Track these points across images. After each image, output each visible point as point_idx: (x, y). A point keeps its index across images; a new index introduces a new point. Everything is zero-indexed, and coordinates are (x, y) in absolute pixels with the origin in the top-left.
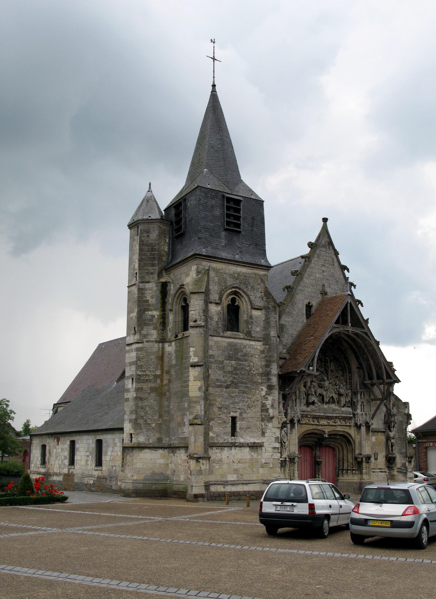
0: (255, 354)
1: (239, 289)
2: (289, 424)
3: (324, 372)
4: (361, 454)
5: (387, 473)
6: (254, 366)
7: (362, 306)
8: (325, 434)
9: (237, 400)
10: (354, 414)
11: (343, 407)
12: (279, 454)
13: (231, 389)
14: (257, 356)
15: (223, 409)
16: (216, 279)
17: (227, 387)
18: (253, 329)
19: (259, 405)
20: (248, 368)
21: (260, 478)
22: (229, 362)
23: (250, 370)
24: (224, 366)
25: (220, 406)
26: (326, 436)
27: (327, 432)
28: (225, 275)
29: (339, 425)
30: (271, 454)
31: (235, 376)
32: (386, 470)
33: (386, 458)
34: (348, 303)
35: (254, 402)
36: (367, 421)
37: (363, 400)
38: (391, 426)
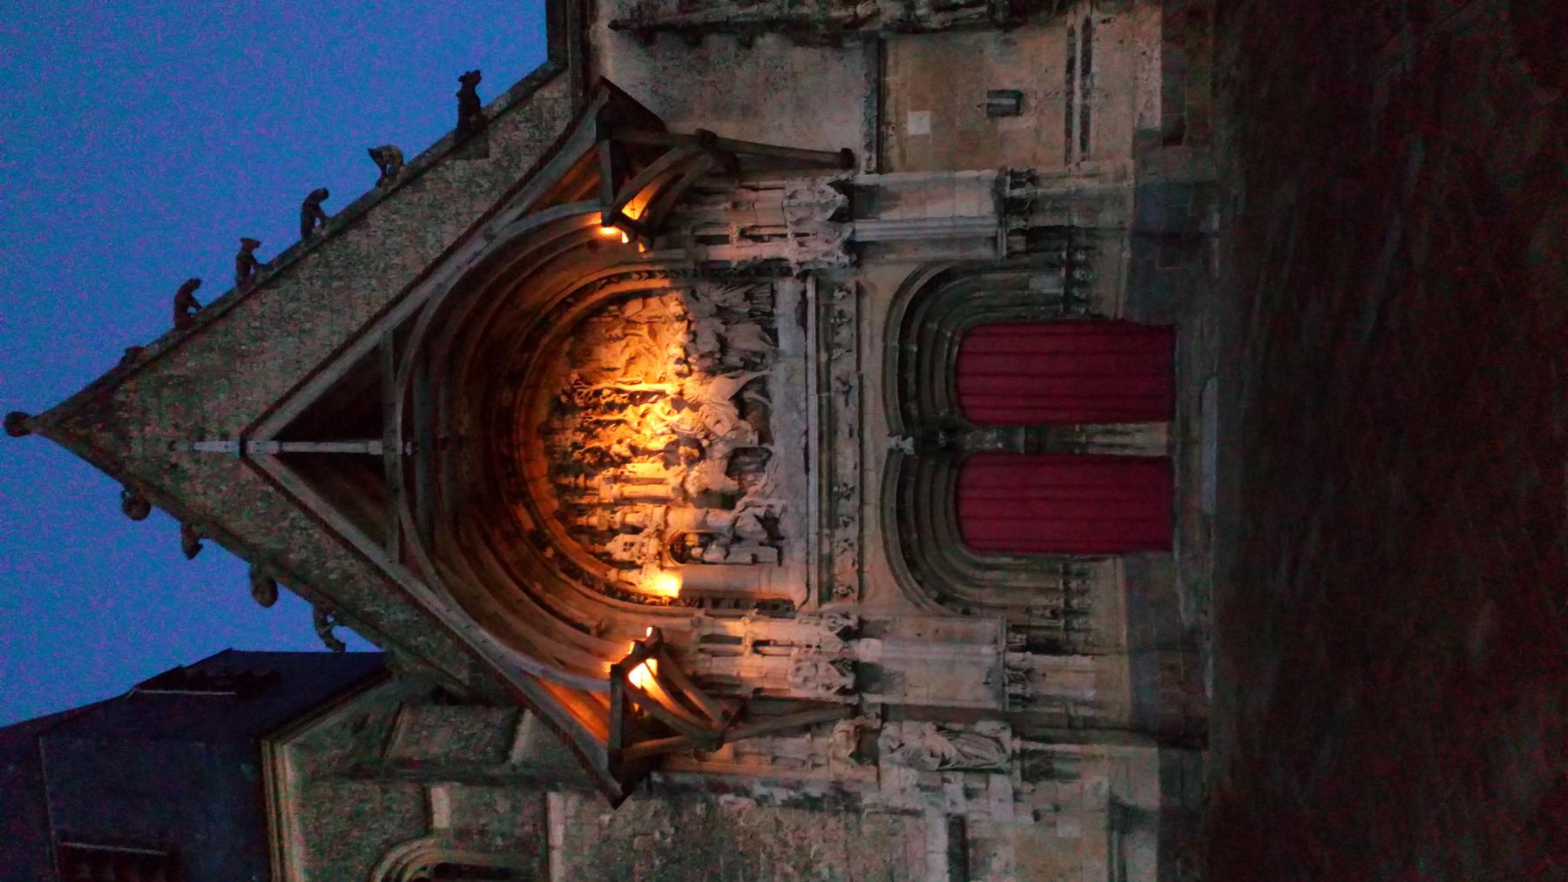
0: (600, 826)
2: (864, 695)
4: (994, 239)
5: (1096, 16)
6: (643, 831)
7: (324, 194)
8: (902, 450)
10: (803, 276)
11: (774, 334)
12: (996, 780)
14: (606, 818)
18: (505, 828)
19: (790, 819)
21: (1103, 838)
26: (908, 445)
27: (893, 442)
29: (859, 368)
30: (994, 803)
32: (1075, 20)
33: (1018, 25)
34: (282, 457)
35: (786, 844)
36: (830, 220)
37: (733, 232)
38: (849, 20)
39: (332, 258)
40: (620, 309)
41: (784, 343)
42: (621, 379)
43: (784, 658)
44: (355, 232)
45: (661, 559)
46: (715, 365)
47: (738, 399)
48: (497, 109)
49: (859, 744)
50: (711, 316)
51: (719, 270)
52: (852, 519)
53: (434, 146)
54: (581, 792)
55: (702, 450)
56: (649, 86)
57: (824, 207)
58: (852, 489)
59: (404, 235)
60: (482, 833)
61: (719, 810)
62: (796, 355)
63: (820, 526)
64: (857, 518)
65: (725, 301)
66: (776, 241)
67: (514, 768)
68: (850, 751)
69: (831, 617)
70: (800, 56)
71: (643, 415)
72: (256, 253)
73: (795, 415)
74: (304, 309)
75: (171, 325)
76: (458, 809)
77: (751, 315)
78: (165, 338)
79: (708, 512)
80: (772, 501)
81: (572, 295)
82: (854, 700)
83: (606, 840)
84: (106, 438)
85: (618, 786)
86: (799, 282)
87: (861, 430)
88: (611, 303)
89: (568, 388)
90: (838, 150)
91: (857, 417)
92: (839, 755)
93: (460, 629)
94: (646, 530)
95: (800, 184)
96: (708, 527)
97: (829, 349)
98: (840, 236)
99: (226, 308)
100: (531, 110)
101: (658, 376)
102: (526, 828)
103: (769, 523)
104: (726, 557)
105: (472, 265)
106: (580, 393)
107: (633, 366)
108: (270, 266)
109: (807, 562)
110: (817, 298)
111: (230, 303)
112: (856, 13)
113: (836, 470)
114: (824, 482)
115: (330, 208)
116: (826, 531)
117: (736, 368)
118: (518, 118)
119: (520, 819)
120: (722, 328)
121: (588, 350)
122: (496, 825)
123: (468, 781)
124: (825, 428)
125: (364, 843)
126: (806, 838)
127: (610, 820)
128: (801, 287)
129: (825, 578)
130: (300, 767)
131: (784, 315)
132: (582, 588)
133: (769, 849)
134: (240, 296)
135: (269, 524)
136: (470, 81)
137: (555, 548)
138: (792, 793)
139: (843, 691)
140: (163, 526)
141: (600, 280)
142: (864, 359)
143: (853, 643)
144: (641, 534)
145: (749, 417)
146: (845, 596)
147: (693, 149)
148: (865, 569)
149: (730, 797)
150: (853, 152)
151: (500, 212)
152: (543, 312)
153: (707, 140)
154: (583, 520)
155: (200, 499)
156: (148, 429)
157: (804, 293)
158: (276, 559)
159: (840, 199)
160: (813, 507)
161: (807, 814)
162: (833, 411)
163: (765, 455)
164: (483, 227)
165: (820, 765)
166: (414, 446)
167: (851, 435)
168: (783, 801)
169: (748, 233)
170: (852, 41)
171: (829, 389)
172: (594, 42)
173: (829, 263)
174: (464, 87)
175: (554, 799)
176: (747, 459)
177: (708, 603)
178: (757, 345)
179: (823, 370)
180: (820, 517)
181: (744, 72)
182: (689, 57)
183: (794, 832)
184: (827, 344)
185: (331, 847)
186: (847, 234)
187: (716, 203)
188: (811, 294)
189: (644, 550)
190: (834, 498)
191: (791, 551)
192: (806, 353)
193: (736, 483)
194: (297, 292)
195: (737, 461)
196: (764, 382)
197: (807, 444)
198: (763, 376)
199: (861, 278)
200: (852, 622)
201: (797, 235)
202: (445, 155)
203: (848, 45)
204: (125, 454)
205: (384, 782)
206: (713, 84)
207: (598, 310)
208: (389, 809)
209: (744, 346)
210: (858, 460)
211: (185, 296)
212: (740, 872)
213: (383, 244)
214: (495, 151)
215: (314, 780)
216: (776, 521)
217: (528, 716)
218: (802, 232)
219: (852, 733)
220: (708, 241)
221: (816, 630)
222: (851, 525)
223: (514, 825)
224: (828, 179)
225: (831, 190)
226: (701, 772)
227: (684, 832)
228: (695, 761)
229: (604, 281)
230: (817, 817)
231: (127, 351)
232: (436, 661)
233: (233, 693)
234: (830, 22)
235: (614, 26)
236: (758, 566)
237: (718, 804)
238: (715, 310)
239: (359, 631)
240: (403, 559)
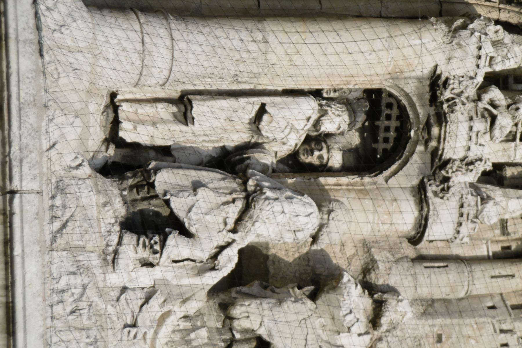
45: (434, 100)
79: (315, 238)
94: (472, 177)
104: (262, 110)
144: (489, 167)
189: (480, 125)
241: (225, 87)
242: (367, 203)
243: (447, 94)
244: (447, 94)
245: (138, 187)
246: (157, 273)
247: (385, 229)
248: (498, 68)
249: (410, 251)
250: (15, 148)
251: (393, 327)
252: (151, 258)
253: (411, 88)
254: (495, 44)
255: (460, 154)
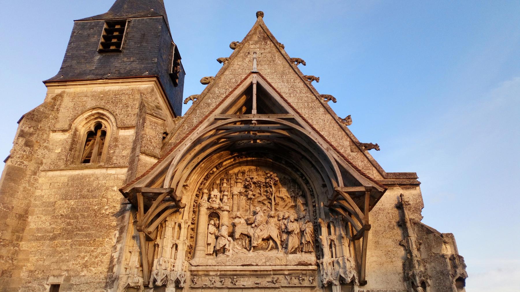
0: (113, 186)
1: (103, 109)
2: (153, 290)
3: (266, 202)
6: (109, 202)
9: (66, 256)
10: (318, 265)
11: (294, 252)
13: (59, 240)
15: (37, 272)
16: (71, 105)
17: (53, 238)
18: (116, 154)
19: (106, 259)
20: (96, 207)
22: (66, 202)
23: (99, 210)
24: (55, 209)
25: (32, 268)
28: (85, 99)
29: (282, 287)
31: (72, 221)
34: (251, 84)
35: (96, 257)
36: (340, 275)
37: (333, 237)
39: (314, 103)
40: (301, 195)
41: (291, 256)
42: (276, 195)
43: (170, 256)
44: (323, 110)
45: (211, 209)
46: (282, 229)
47: (270, 238)
48: (368, 155)
49: (133, 288)
50: (300, 228)
51: (317, 231)
52: (223, 285)
53: (353, 136)
54: (126, 180)
55: (251, 224)
56: (381, 207)
57: (345, 273)
58: (235, 284)
59: (323, 125)
60: (116, 146)
61: (113, 230)
62: (287, 262)
63: (221, 271)
64: (224, 286)
65: (306, 233)
66: (330, 254)
67: (138, 156)
68: (130, 284)
69: (185, 275)
70: (399, 264)
71: (263, 203)
72: (315, 81)
73: (264, 261)
74: (297, 95)
75: (291, 56)
76: (125, 138)
77: (301, 243)
78: (287, 55)
80: (231, 251)
81: (306, 178)
82: (151, 285)
83: (107, 189)
84: (255, 38)
85: (128, 190)
86: (315, 262)
87: (258, 288)
88: (303, 192)
89: (273, 176)
90: (366, 280)
91: (263, 286)
92: (129, 279)
93: (191, 137)
94: (221, 204)
95: (353, 263)
96: (221, 226)
97: (289, 275)
98: (334, 280)
99: (297, 73)
100: (369, 166)
101: (277, 209)
102: (115, 161)
103: (223, 250)
104: (210, 233)
105: (318, 143)
106: (271, 181)
107: (281, 200)
108: (311, 85)
109: (207, 265)
110: (309, 270)
111: (299, 73)
112: (418, 287)
113: (242, 277)
114: (238, 273)
115: (330, 103)
116: (219, 273)
117: (281, 238)
118: (365, 162)
119: (119, 158)
120: (296, 232)
121: (286, 184)
122: (117, 151)
123: (135, 142)
124: (259, 273)
125: (117, 108)
126: (97, 265)
127: (114, 190)
128: (313, 263)
129: (200, 273)
130: (146, 89)
131: (302, 255)
132: (201, 180)
133: (95, 250)
134: (301, 77)
135: (228, 82)
136: (376, 147)
137: (216, 171)
138: (116, 260)
139: (155, 281)
140: (228, 53)
141: (312, 188)
142: (286, 289)
143: (174, 285)
145: (263, 242)
146: (193, 281)
147: (364, 222)
148: (203, 290)
149: (117, 235)
150: (366, 285)
151: (336, 152)
152: (299, 169)
153: (367, 227)
154: (225, 181)
155: (236, 63)
156: (259, 50)
157: (311, 265)
158: (215, 84)
159: (349, 280)
160: (228, 268)
161: (107, 266)
162: (265, 276)
163: (248, 249)
164: (331, 147)
165: (126, 271)
166: (255, 124)
167: (257, 284)
168: (113, 256)
169: (333, 243)
170: (407, 286)
171: (274, 274)
172: (395, 188)
173: (323, 275)
174: (374, 145)
175: (125, 170)
176: (247, 242)
177: (193, 226)
178: (290, 246)
179: (281, 272)
180: (225, 271)
181: (390, 242)
182: (394, 223)
183: (101, 261)
184: (292, 274)
185: (117, 98)
186: (334, 282)
187: (343, 230)
188: (310, 267)
189: (214, 202)
190: (232, 277)
191: (211, 259)
192: (288, 265)
193: (238, 237)
194: (303, 93)
195: (246, 238)
196: (276, 248)
197: (253, 265)
198: (278, 248)
199: (317, 288)
200: (182, 285)
201: (333, 262)
202: (350, 138)
203: (405, 284)
204: (251, 43)
205: (138, 114)
206: (385, 231)
207: (300, 187)
208: (128, 116)
209: (290, 241)
210: (246, 287)
211: (300, 61)
212: (88, 239)
213: (320, 119)
214: (353, 154)
215: (141, 93)
216: (224, 253)
217: (155, 161)
218: (334, 264)
219: (138, 284)
220: (329, 227)
221: (180, 269)
222: (221, 284)
223: (117, 156)
224: (355, 275)
225: (352, 276)
226: (129, 223)
227: (106, 217)
228: (133, 221)
229: (311, 189)
230: (105, 270)
231: (283, 45)
232: (178, 132)
233: (172, 72)
234: (414, 276)
235: (401, 195)
236: (206, 245)
237: (115, 230)
238: (303, 230)
239: (191, 108)
240: (216, 120)
241: (206, 238)
242: (223, 218)
243: (210, 207)
244: (210, 207)
245: (219, 251)
246: (230, 249)
247: (227, 216)
248: (207, 200)
249: (231, 212)
250: (212, 269)
251: (241, 215)
252: (228, 250)
253: (208, 212)
254: (204, 200)
255: (218, 205)
